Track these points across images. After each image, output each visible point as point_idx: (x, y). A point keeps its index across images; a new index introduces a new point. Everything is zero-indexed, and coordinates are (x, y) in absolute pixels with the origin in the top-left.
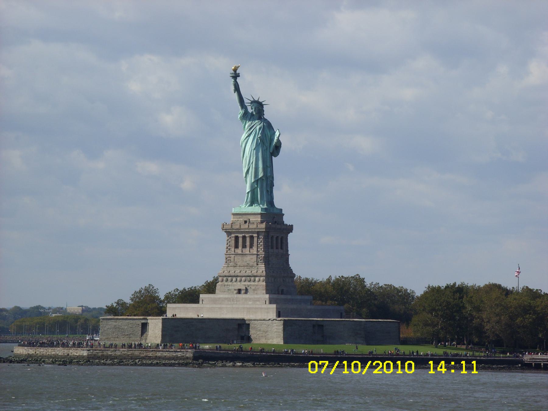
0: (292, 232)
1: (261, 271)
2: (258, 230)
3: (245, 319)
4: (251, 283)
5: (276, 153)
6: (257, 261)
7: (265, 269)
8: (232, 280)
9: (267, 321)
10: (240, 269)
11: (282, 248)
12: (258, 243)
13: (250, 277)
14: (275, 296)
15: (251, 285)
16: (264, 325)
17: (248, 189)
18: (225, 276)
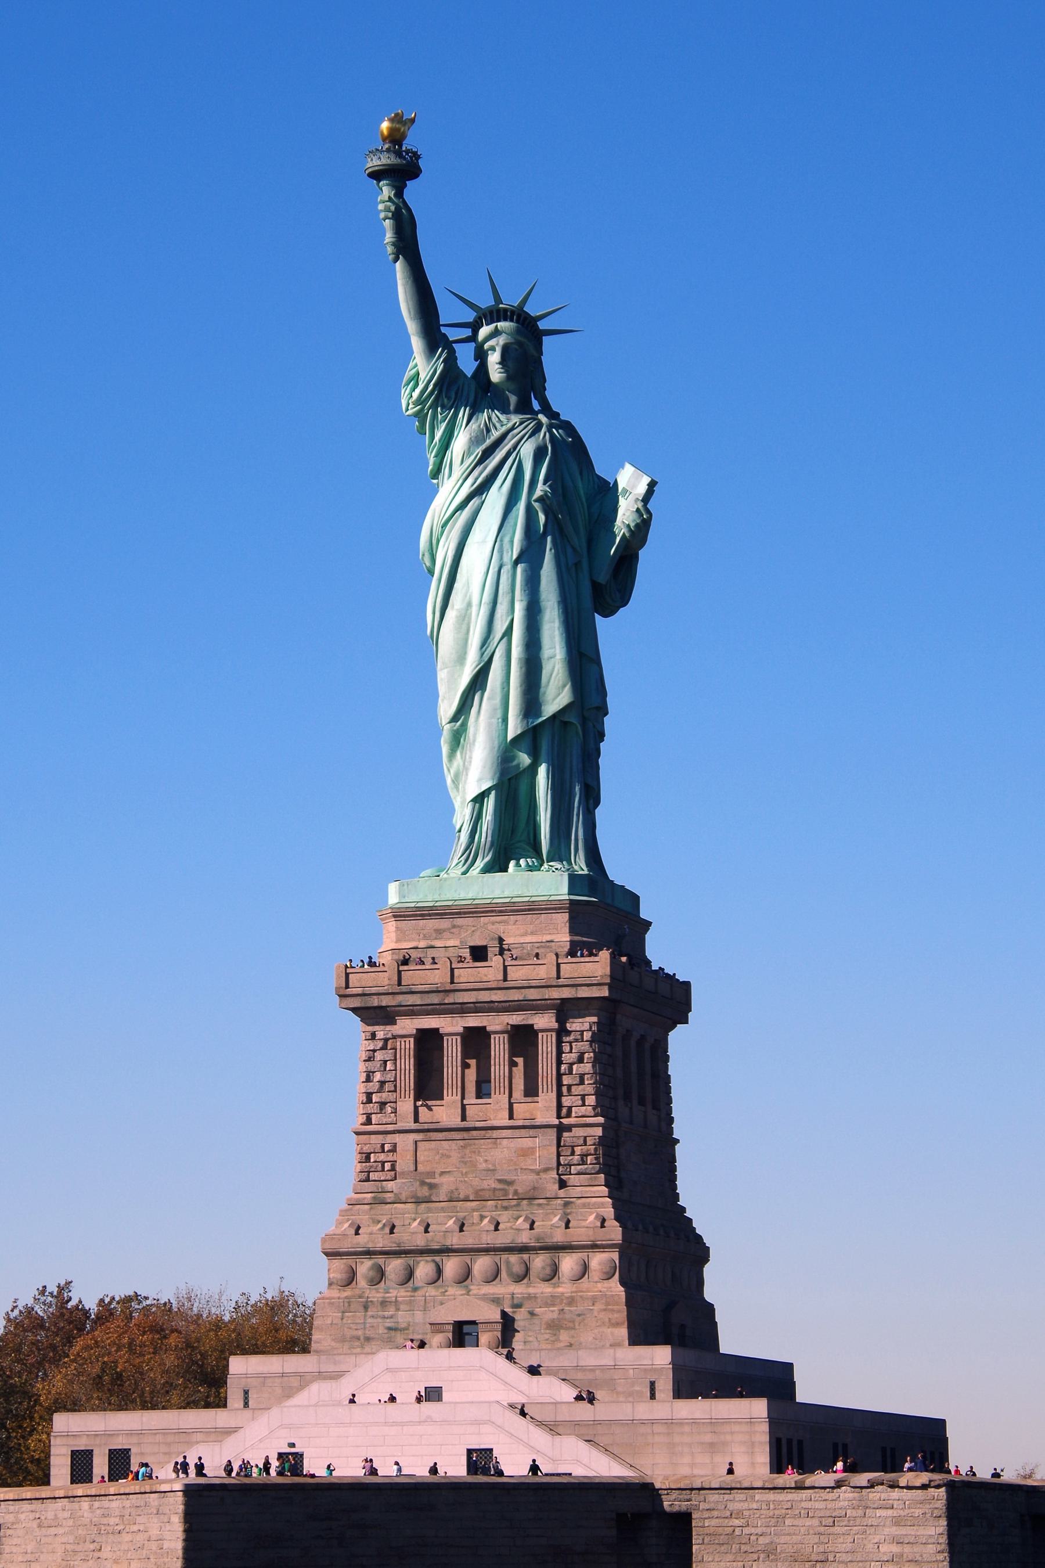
0: (686, 1022)
1: (592, 1218)
2: (566, 993)
3: (657, 1486)
4: (531, 1290)
6: (559, 1164)
7: (614, 1206)
8: (410, 1274)
9: (824, 1494)
10: (454, 1210)
11: (656, 1107)
12: (563, 1067)
13: (525, 1256)
14: (690, 1355)
15: (530, 1297)
16: (798, 1522)
17: (480, 780)
18: (369, 1253)
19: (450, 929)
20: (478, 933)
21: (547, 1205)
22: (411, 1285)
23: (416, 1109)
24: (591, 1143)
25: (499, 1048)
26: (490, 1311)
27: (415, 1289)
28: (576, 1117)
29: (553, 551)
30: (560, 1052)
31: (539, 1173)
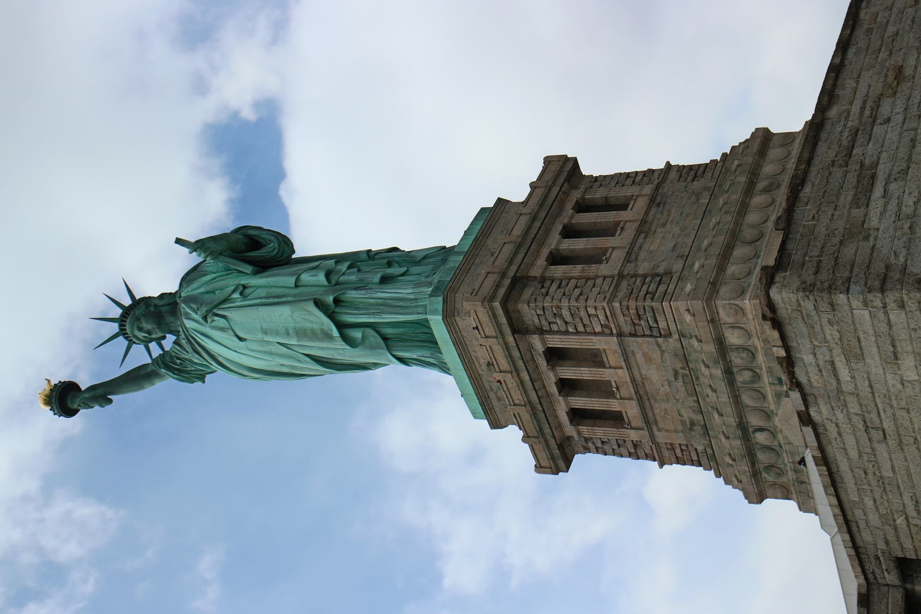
2: (507, 330)
5: (272, 244)
6: (651, 336)
8: (769, 448)
12: (571, 330)
13: (735, 370)
18: (755, 474)
19: (495, 393)
20: (489, 378)
21: (687, 349)
22: (778, 448)
23: (632, 428)
24: (627, 312)
25: (569, 372)
26: (787, 405)
27: (780, 446)
28: (609, 321)
29: (232, 312)
30: (559, 332)
31: (662, 351)
